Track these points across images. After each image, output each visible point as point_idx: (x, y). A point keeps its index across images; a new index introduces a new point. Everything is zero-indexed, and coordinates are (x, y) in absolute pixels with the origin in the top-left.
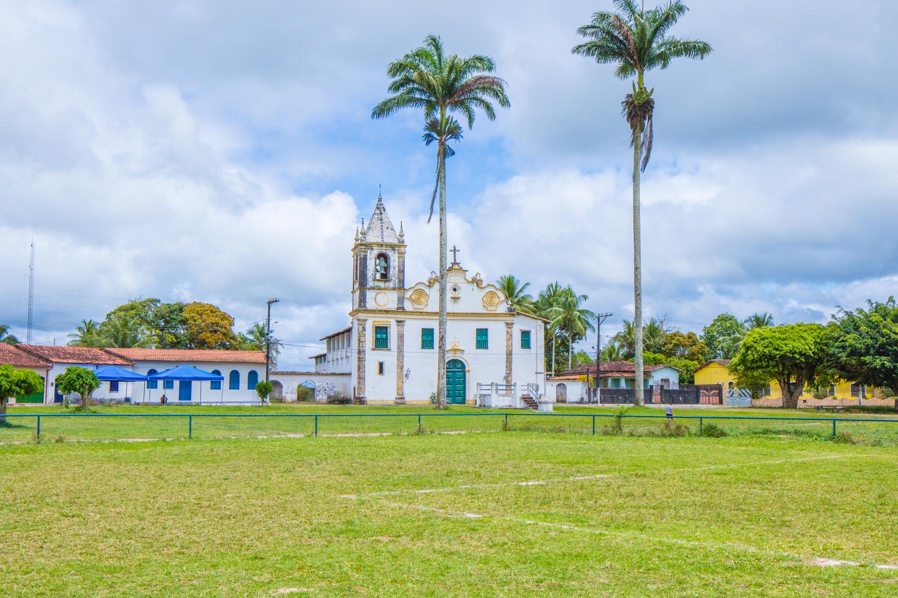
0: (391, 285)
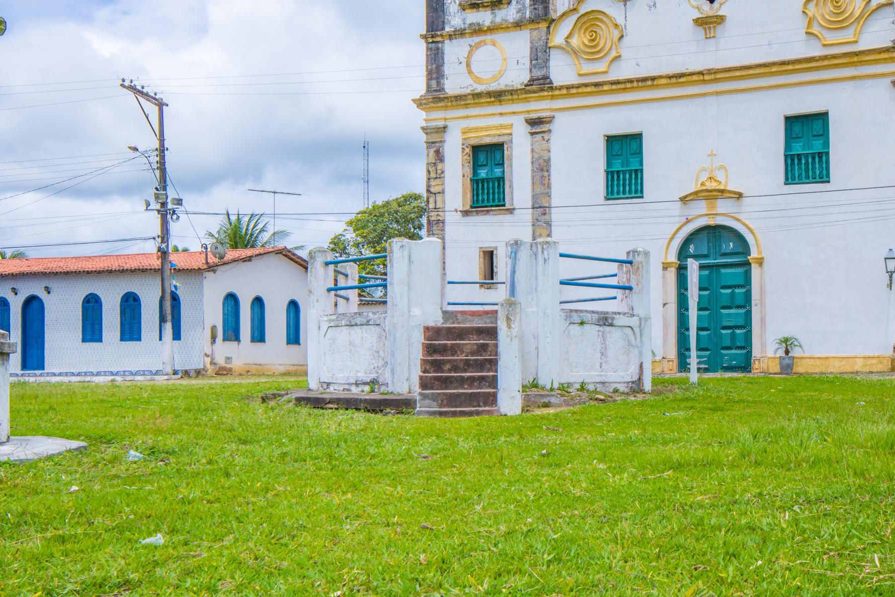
0: (509, 13)
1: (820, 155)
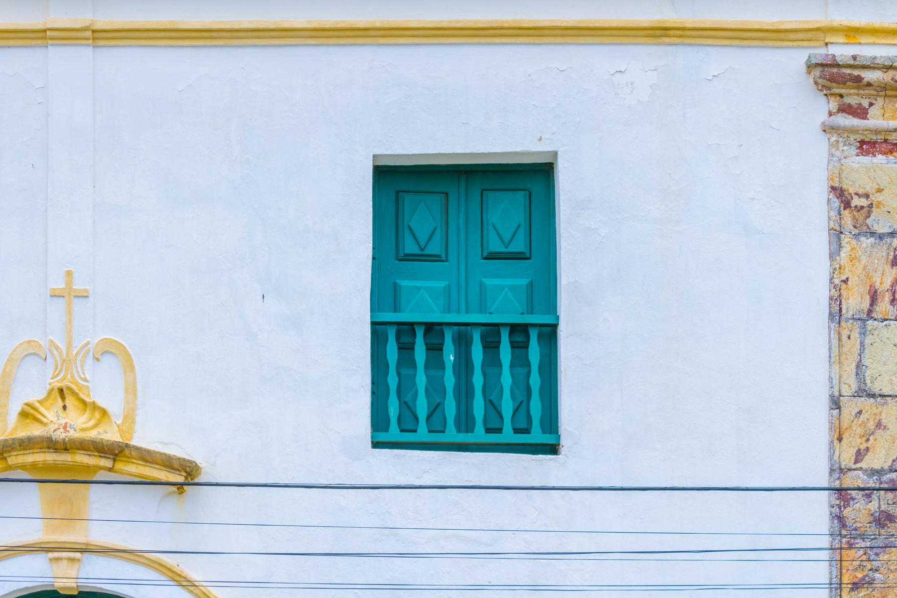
1: (519, 330)
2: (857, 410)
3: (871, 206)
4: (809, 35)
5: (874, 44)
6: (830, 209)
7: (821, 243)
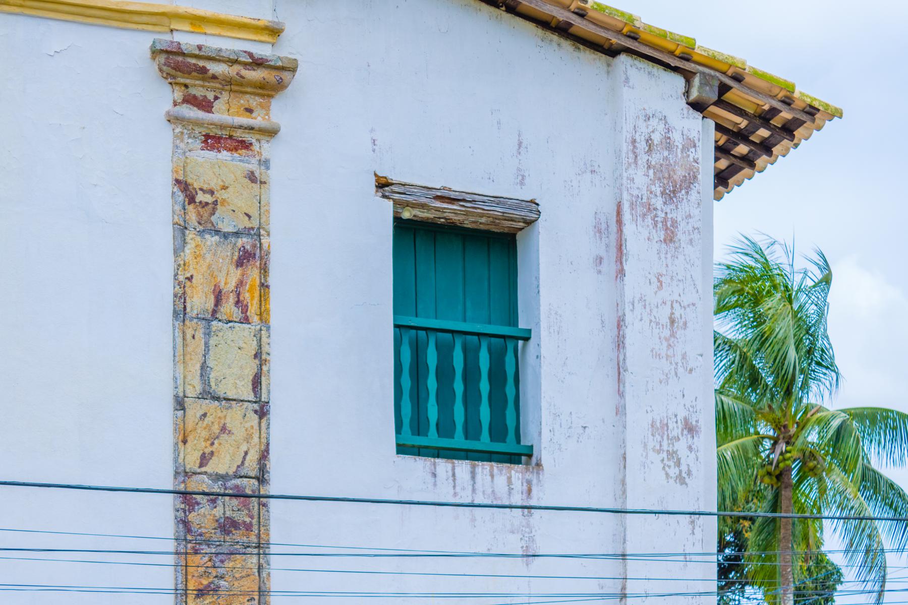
2: (202, 412)
3: (215, 203)
4: (154, 19)
5: (220, 36)
6: (175, 203)
7: (165, 237)
